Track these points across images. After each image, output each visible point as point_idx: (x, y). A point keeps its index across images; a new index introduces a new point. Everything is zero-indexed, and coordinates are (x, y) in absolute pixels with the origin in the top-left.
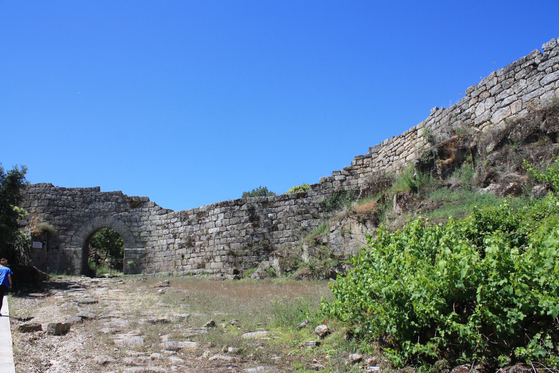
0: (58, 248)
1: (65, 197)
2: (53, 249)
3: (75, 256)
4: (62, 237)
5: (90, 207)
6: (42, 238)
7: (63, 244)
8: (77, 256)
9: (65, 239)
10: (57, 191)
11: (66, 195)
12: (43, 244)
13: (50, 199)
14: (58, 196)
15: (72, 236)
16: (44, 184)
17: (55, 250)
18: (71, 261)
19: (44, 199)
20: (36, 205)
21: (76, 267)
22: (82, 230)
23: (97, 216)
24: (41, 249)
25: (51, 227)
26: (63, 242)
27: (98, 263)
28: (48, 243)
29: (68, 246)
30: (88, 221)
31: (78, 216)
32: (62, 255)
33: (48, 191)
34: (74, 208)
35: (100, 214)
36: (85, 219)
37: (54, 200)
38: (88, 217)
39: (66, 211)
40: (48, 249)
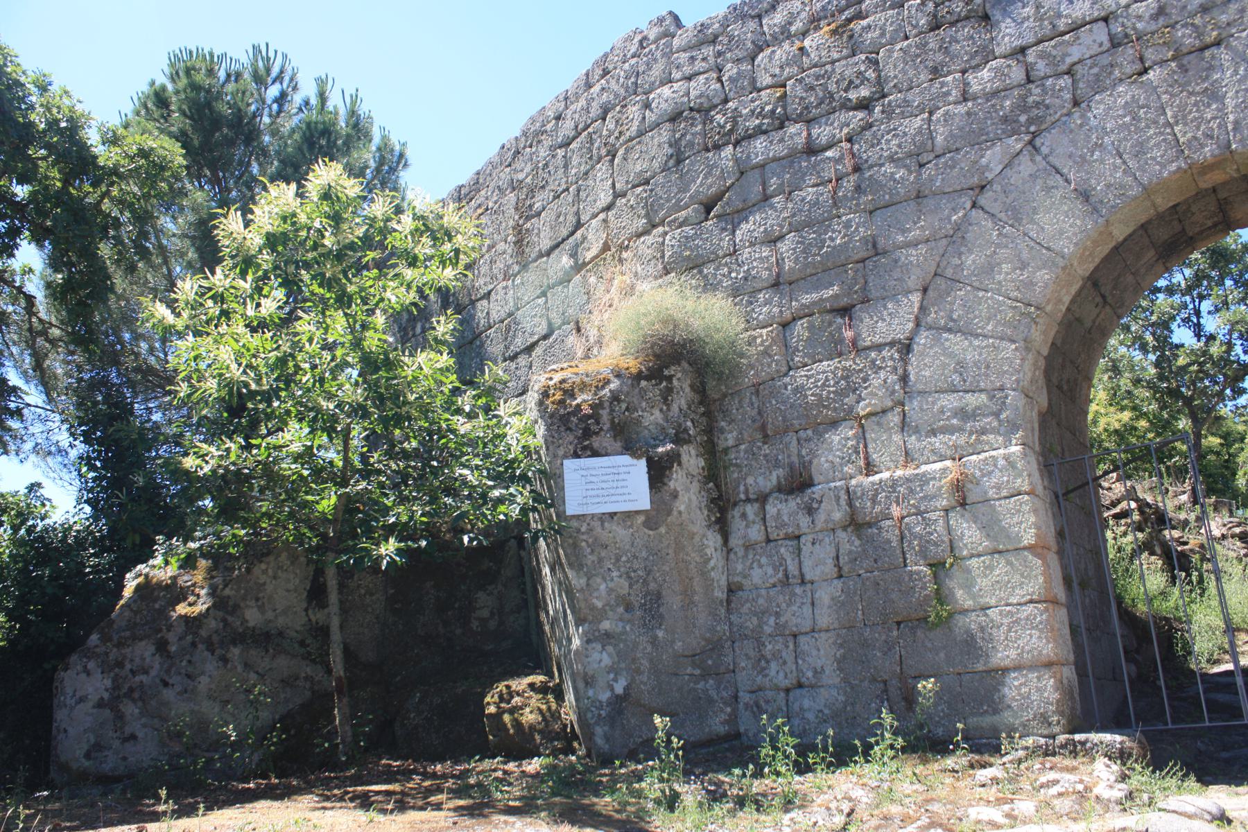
0: (799, 483)
1: (784, 51)
2: (762, 499)
3: (969, 533)
4: (816, 376)
5: (1008, 34)
6: (652, 418)
7: (841, 438)
8: (990, 526)
9: (850, 386)
10: (714, 40)
11: (785, 33)
12: (658, 472)
13: (675, 118)
14: (730, 70)
15: (906, 348)
16: (629, 39)
17: (783, 509)
18: (941, 596)
19: (641, 134)
20: (604, 198)
21: (1004, 655)
22: (990, 268)
23: (1098, 86)
24: (652, 519)
25: (710, 314)
26: (834, 424)
27: (1177, 563)
28: (711, 451)
29: (886, 445)
30: (1026, 166)
31: (919, 156)
32: (848, 542)
33: (657, 71)
34: (864, 105)
35: (1126, 59)
36: (993, 157)
37: (704, 111)
38: (1010, 124)
39: (811, 150)
40: (721, 508)
